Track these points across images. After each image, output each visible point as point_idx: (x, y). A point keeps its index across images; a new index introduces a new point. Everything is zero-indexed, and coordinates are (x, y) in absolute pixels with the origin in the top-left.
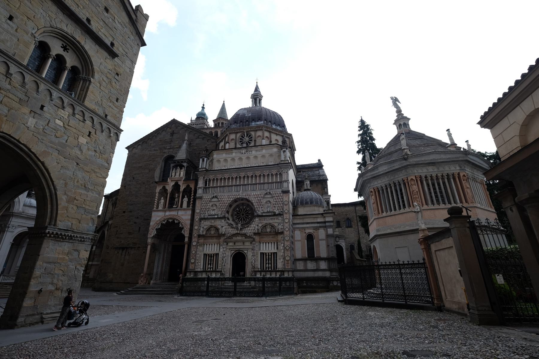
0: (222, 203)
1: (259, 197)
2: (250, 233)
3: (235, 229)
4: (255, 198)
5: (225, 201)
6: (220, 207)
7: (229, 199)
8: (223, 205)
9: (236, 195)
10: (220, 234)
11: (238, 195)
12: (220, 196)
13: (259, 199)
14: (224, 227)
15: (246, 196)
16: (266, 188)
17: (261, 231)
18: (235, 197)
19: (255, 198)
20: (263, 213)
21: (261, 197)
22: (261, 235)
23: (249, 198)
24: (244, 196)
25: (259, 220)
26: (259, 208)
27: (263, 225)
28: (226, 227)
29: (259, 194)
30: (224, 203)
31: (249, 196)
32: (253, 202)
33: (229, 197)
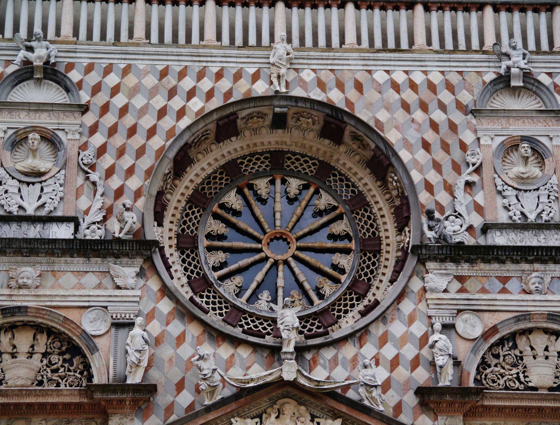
0: (113, 131)
1: (443, 107)
2: (386, 386)
3: (244, 353)
4: (406, 106)
5: (143, 111)
6: (88, 156)
7: (177, 103)
8: (118, 140)
9: (238, 76)
10: (103, 388)
11: (256, 77)
12: (89, 69)
13: (438, 116)
14: (137, 331)
15: (322, 85)
16: (490, 40)
17: (476, 380)
18: (225, 84)
19: (406, 106)
20: (486, 229)
21: (460, 106)
22: (489, 411)
23: (349, 103)
24: (303, 84)
25: (457, 285)
26: (452, 194)
27: (494, 330)
28: (155, 328)
29: (436, 78)
30: (132, 131)
31: (352, 94)
32: (392, 136)
33: (171, 81)
